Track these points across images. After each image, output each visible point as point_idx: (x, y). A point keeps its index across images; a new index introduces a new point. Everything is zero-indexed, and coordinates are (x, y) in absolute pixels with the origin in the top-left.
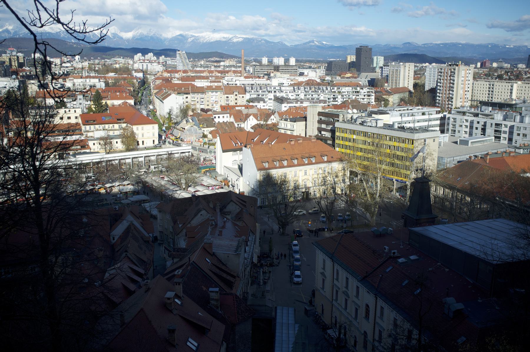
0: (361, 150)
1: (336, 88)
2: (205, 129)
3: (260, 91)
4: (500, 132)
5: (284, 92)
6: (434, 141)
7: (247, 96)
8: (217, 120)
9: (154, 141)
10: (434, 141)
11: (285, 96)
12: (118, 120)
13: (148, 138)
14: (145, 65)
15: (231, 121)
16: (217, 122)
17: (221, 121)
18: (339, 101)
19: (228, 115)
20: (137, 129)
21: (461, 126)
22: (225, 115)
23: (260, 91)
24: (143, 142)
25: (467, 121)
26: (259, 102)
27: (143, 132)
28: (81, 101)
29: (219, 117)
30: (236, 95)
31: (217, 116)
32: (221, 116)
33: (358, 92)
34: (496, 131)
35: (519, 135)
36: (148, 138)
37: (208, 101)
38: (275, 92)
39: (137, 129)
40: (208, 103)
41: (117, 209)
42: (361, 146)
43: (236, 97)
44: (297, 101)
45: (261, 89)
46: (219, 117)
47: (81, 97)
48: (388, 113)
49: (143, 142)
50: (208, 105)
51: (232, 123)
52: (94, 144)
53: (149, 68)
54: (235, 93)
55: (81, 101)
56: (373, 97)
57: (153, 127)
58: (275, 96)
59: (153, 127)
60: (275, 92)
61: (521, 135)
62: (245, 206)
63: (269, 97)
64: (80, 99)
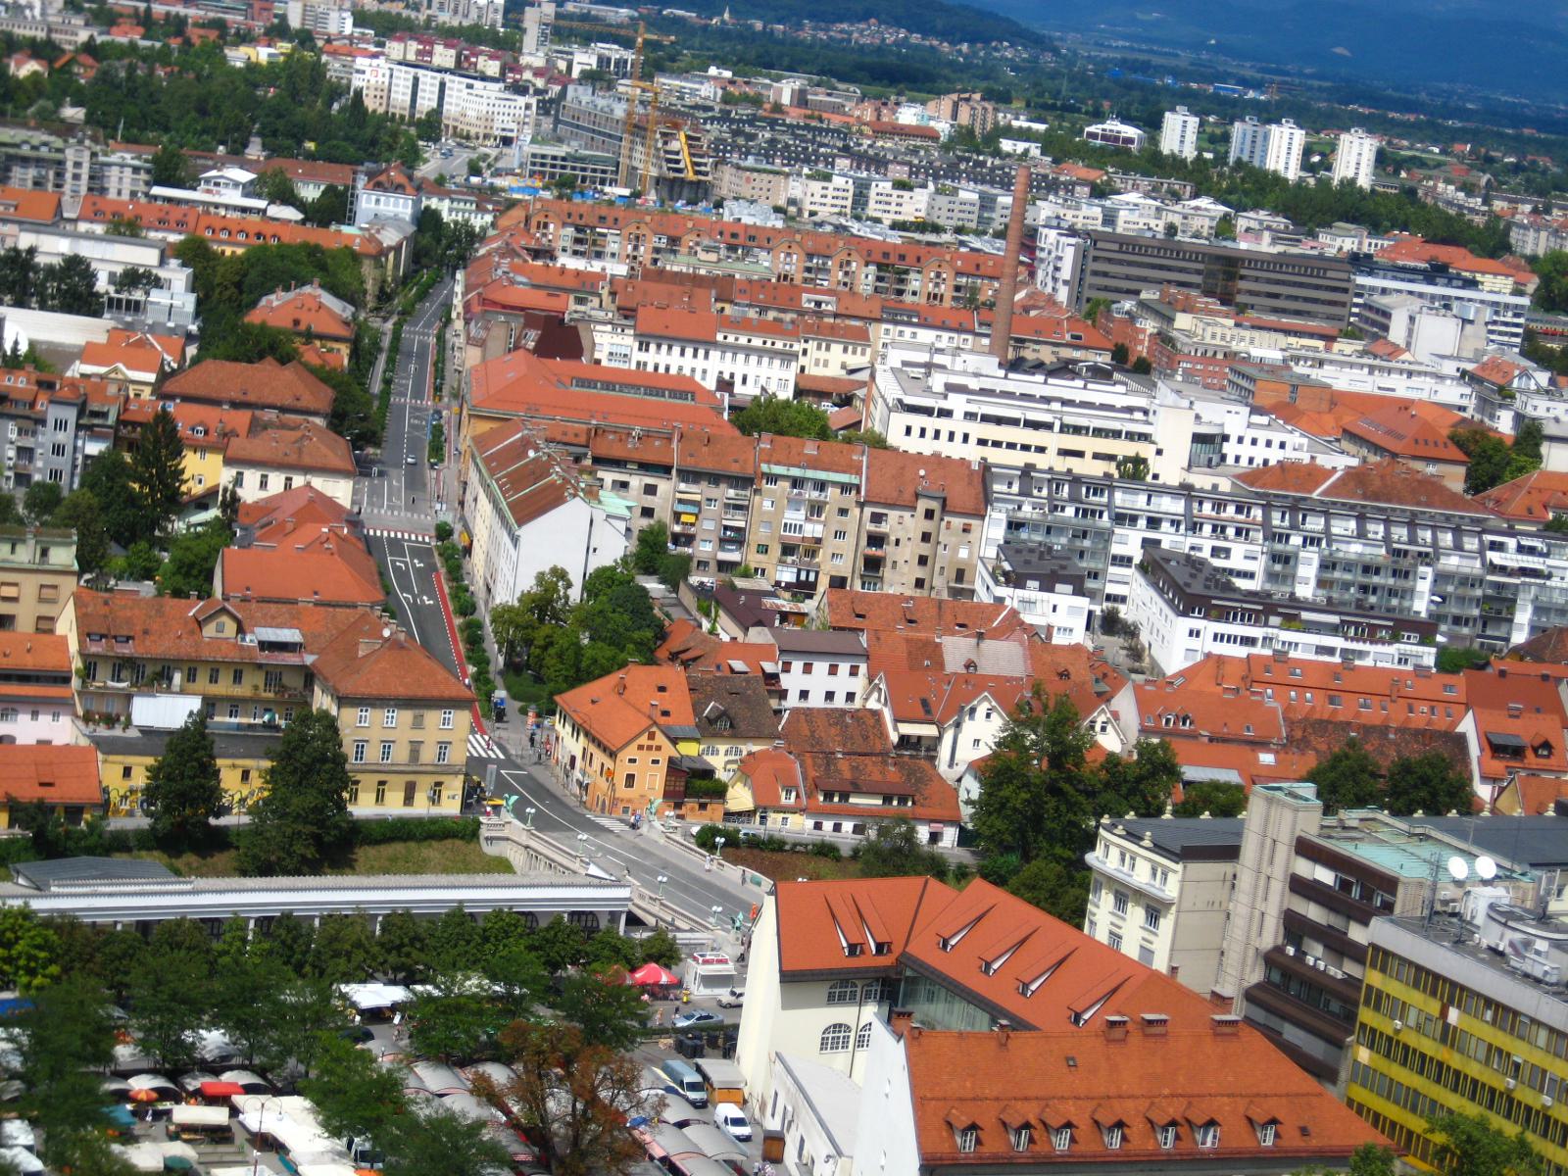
0: (1474, 1089)
5: (1207, 529)
8: (792, 681)
11: (1206, 554)
14: (429, 82)
15: (873, 704)
17: (816, 701)
23: (1070, 511)
26: (1047, 586)
28: (61, 437)
30: (929, 514)
42: (1474, 1070)
43: (928, 526)
44: (1262, 608)
45: (1074, 498)
47: (70, 415)
53: (450, 109)
54: (923, 505)
55: (61, 437)
60: (1154, 523)
63: (1116, 549)
64: (61, 425)
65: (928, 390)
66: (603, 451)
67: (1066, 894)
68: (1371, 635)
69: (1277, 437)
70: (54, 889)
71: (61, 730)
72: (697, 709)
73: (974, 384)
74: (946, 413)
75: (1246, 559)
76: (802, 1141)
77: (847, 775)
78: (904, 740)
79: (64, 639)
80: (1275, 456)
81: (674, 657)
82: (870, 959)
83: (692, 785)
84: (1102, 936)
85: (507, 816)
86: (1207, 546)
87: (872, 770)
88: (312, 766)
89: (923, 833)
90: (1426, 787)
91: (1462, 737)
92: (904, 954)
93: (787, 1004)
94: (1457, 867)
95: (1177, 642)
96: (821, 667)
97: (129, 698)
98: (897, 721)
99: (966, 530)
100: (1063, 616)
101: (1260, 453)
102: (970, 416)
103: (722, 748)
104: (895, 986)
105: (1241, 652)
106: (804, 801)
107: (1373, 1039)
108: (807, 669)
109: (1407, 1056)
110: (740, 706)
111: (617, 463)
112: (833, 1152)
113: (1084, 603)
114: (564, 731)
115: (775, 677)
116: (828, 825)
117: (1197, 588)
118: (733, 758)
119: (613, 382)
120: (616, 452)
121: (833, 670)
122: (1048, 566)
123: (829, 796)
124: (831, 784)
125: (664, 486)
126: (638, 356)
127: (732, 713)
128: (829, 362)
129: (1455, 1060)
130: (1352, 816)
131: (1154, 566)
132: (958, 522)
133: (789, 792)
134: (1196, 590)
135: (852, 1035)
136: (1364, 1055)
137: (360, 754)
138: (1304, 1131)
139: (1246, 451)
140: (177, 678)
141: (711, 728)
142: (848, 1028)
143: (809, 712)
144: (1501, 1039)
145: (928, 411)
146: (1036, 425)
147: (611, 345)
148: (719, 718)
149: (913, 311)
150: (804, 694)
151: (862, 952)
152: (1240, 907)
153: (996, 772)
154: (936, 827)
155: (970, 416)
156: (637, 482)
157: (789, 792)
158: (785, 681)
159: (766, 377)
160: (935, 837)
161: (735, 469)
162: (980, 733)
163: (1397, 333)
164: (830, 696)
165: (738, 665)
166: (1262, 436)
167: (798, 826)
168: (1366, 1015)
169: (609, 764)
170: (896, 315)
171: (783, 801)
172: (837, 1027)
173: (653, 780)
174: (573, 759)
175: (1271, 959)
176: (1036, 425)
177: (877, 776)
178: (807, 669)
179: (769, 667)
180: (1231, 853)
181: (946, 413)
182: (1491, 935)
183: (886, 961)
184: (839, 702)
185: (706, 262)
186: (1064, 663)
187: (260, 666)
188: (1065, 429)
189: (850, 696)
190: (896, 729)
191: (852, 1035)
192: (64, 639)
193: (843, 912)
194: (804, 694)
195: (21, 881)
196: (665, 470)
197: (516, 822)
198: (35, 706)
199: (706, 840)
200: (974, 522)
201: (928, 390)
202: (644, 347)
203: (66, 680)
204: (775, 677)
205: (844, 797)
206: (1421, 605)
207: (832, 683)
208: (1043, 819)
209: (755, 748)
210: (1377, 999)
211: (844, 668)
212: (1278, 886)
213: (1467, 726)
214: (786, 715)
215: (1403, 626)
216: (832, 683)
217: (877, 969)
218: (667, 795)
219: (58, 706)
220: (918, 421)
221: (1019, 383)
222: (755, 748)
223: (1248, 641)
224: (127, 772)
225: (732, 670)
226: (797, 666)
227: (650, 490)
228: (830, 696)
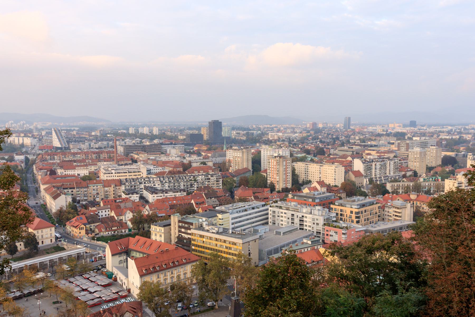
1: (192, 177)
2: (92, 225)
3: (133, 183)
4: (303, 221)
6: (255, 241)
7: (123, 188)
8: (100, 214)
9: (51, 240)
10: (255, 241)
14: (21, 139)
15: (112, 215)
16: (101, 217)
17: (104, 216)
18: (195, 186)
19: (109, 210)
20: (38, 233)
21: (279, 216)
22: (107, 210)
24: (42, 242)
25: (282, 213)
26: (132, 194)
27: (42, 234)
29: (102, 212)
31: (100, 211)
32: (104, 211)
33: (209, 179)
34: (300, 220)
35: (314, 223)
36: (47, 238)
37: (90, 193)
38: (145, 183)
39: (38, 233)
40: (90, 195)
44: (162, 191)
45: (133, 181)
46: (102, 212)
48: (227, 212)
49: (42, 242)
50: (91, 197)
51: (113, 216)
53: (25, 142)
56: (221, 182)
57: (51, 230)
58: (145, 186)
59: (51, 230)
60: (145, 183)
61: (316, 224)
62: (135, 312)
63: (141, 187)
65: (109, 171)
66: (64, 187)
67: (147, 235)
68: (177, 192)
69: (158, 168)
72: (88, 220)
73: (115, 168)
74: (112, 173)
75: (158, 186)
80: (158, 171)
84: (154, 239)
86: (153, 184)
89: (123, 231)
90: (191, 211)
91: (192, 203)
94: (200, 220)
95: (151, 198)
99: (119, 189)
100: (135, 197)
101: (156, 171)
102: (115, 173)
104: (127, 252)
105: (161, 198)
107: (194, 245)
109: (199, 246)
110: (93, 219)
111: (67, 189)
113: (138, 195)
116: (110, 233)
117: (153, 190)
119: (62, 177)
120: (66, 187)
121: (105, 211)
122: (132, 192)
125: (74, 190)
126: (64, 173)
128: (93, 168)
129: (205, 245)
130: (184, 216)
131: (146, 188)
132: (118, 187)
134: (154, 191)
136: (193, 247)
137: (38, 237)
138: (189, 260)
139: (154, 171)
141: (89, 223)
143: (104, 218)
144: (211, 241)
145: (109, 173)
146: (125, 173)
147: (60, 171)
149: (102, 160)
152: (172, 232)
153: (133, 221)
155: (115, 173)
156: (70, 191)
158: (99, 214)
159: (83, 172)
161: (84, 186)
162: (129, 215)
163: (168, 152)
165: (92, 214)
166: (156, 169)
167: (106, 234)
168: (193, 242)
170: (100, 160)
173: (83, 232)
175: (178, 237)
176: (125, 173)
179: (96, 213)
180: (170, 225)
181: (112, 173)
182: (207, 228)
184: (107, 216)
185: (71, 158)
186: (138, 204)
188: (129, 172)
189: (109, 215)
196: (74, 188)
199: (93, 239)
200: (120, 187)
201: (109, 171)
202: (65, 172)
204: (97, 214)
206: (182, 187)
208: (142, 226)
210: (194, 240)
212: (177, 228)
213: (193, 202)
215: (181, 191)
220: (108, 175)
221: (121, 167)
223: (161, 196)
226: (100, 211)
227: (72, 191)
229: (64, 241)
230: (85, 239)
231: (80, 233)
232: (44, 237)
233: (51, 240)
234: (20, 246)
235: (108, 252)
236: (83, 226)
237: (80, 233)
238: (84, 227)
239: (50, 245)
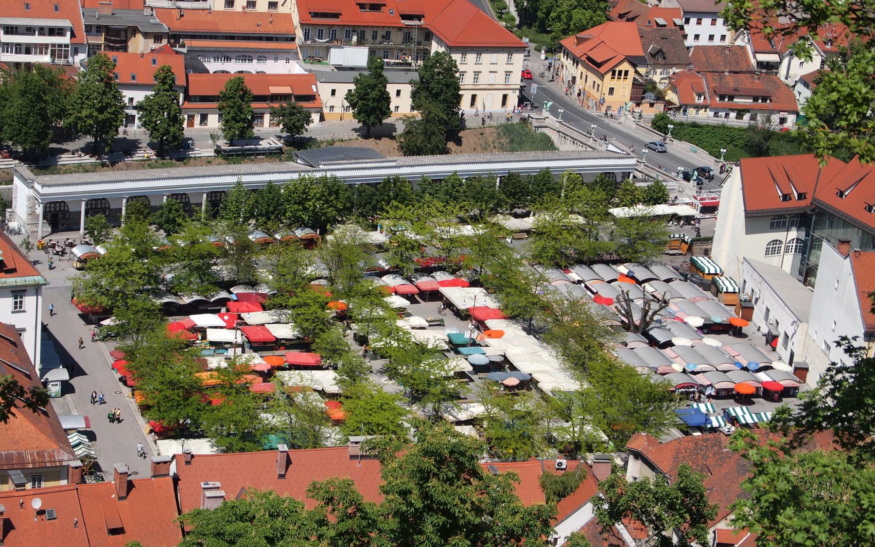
8: (691, 29)
9: (505, 97)
12: (405, 17)
13: (491, 88)
24: (474, 97)
27: (478, 68)
36: (491, 88)
41: (564, 466)
49: (474, 97)
52: (333, 92)
70: (321, 167)
71: (296, 68)
72: (645, 47)
76: (768, 310)
77: (732, 85)
78: (760, 64)
79: (289, 16)
81: (621, 16)
82: (795, 203)
83: (642, 91)
85: (545, 113)
87: (745, 82)
88: (440, 89)
92: (814, 199)
93: (749, 230)
96: (707, 21)
97: (328, 49)
98: (755, 53)
103: (659, 71)
106: (709, 101)
108: (699, 23)
112: (796, 319)
114: (568, 62)
115: (682, 28)
118: (664, 76)
123: (722, 98)
124: (723, 91)
127: (664, 50)
133: (700, 96)
135: (783, 246)
140: (355, 38)
142: (781, 242)
148: (657, 53)
150: (697, 37)
151: (790, 199)
154: (782, 115)
157: (700, 96)
160: (783, 121)
164: (711, 37)
165: (661, 21)
167: (705, 117)
169: (598, 81)
171: (697, 101)
172: (775, 241)
173: (624, 88)
174: (574, 78)
177: (748, 86)
178: (699, 23)
179: (679, 22)
183: (803, 203)
184: (717, 42)
187: (400, 29)
190: (755, 57)
191: (783, 246)
192: (289, 16)
193: (780, 177)
194: (697, 37)
195: (299, 161)
197: (551, 117)
198: (276, 55)
203: (293, 39)
205: (731, 98)
207: (713, 30)
209: (677, 71)
211: (720, 21)
214: (692, 50)
216: (713, 30)
217: (799, 209)
218: (631, 99)
219: (288, 55)
222: (677, 71)
224: (333, 92)
225: (657, 24)
226: (693, 21)
228: (711, 37)
229: (553, 111)
230: (627, 123)
231: (611, 90)
232: (484, 79)
233: (505, 97)
234: (402, 102)
235: (731, 195)
236: (625, 66)
237: (611, 90)
238: (631, 71)
239: (500, 115)
